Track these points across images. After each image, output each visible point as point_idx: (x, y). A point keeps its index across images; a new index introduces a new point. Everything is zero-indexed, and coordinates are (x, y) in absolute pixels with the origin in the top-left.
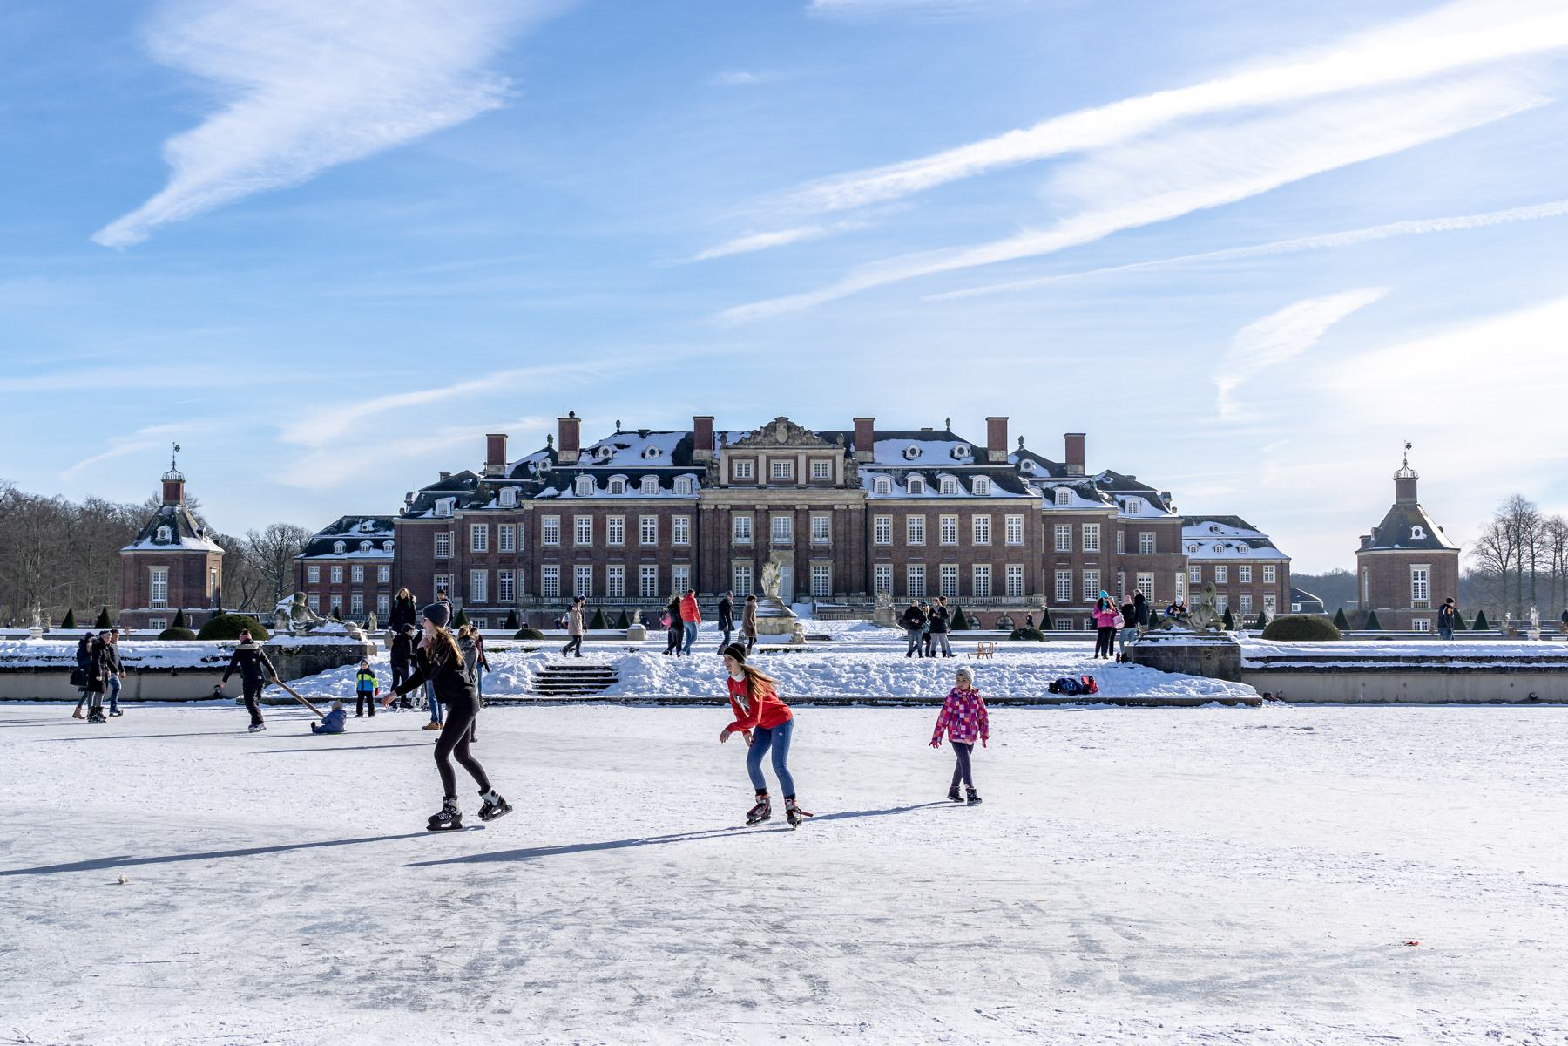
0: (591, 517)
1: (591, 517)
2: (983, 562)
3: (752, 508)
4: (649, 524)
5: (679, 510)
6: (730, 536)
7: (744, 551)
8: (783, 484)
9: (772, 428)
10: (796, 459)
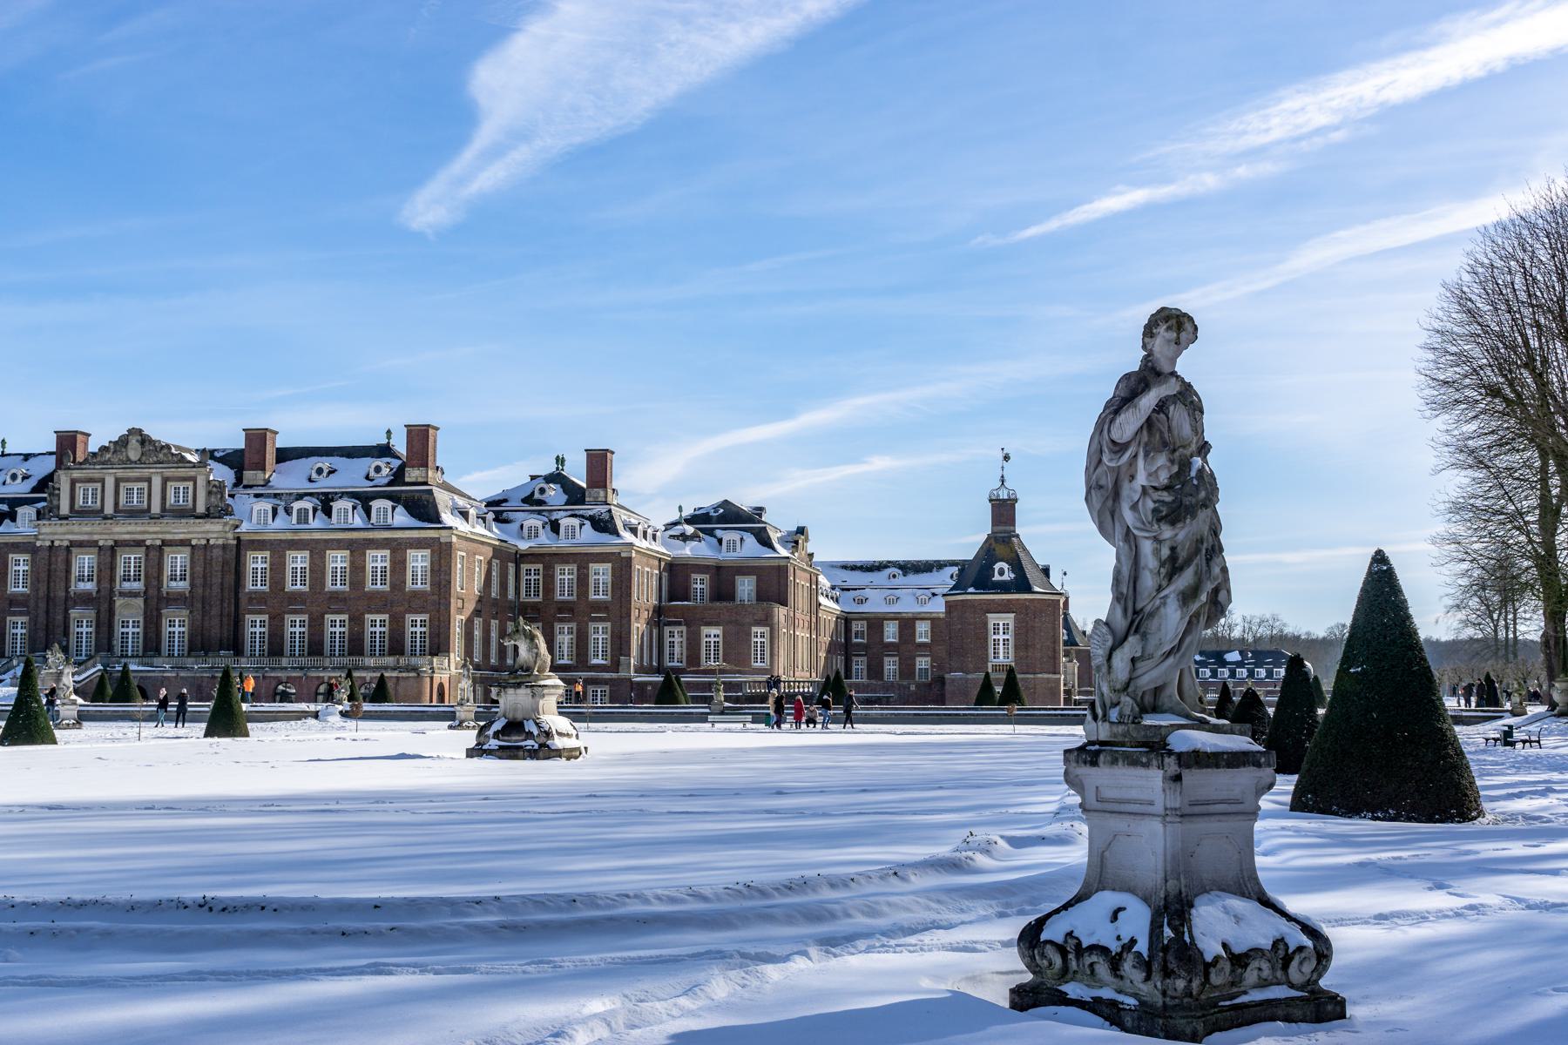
2: (378, 612)
3: (94, 544)
6: (68, 580)
7: (85, 599)
9: (122, 443)
10: (149, 481)
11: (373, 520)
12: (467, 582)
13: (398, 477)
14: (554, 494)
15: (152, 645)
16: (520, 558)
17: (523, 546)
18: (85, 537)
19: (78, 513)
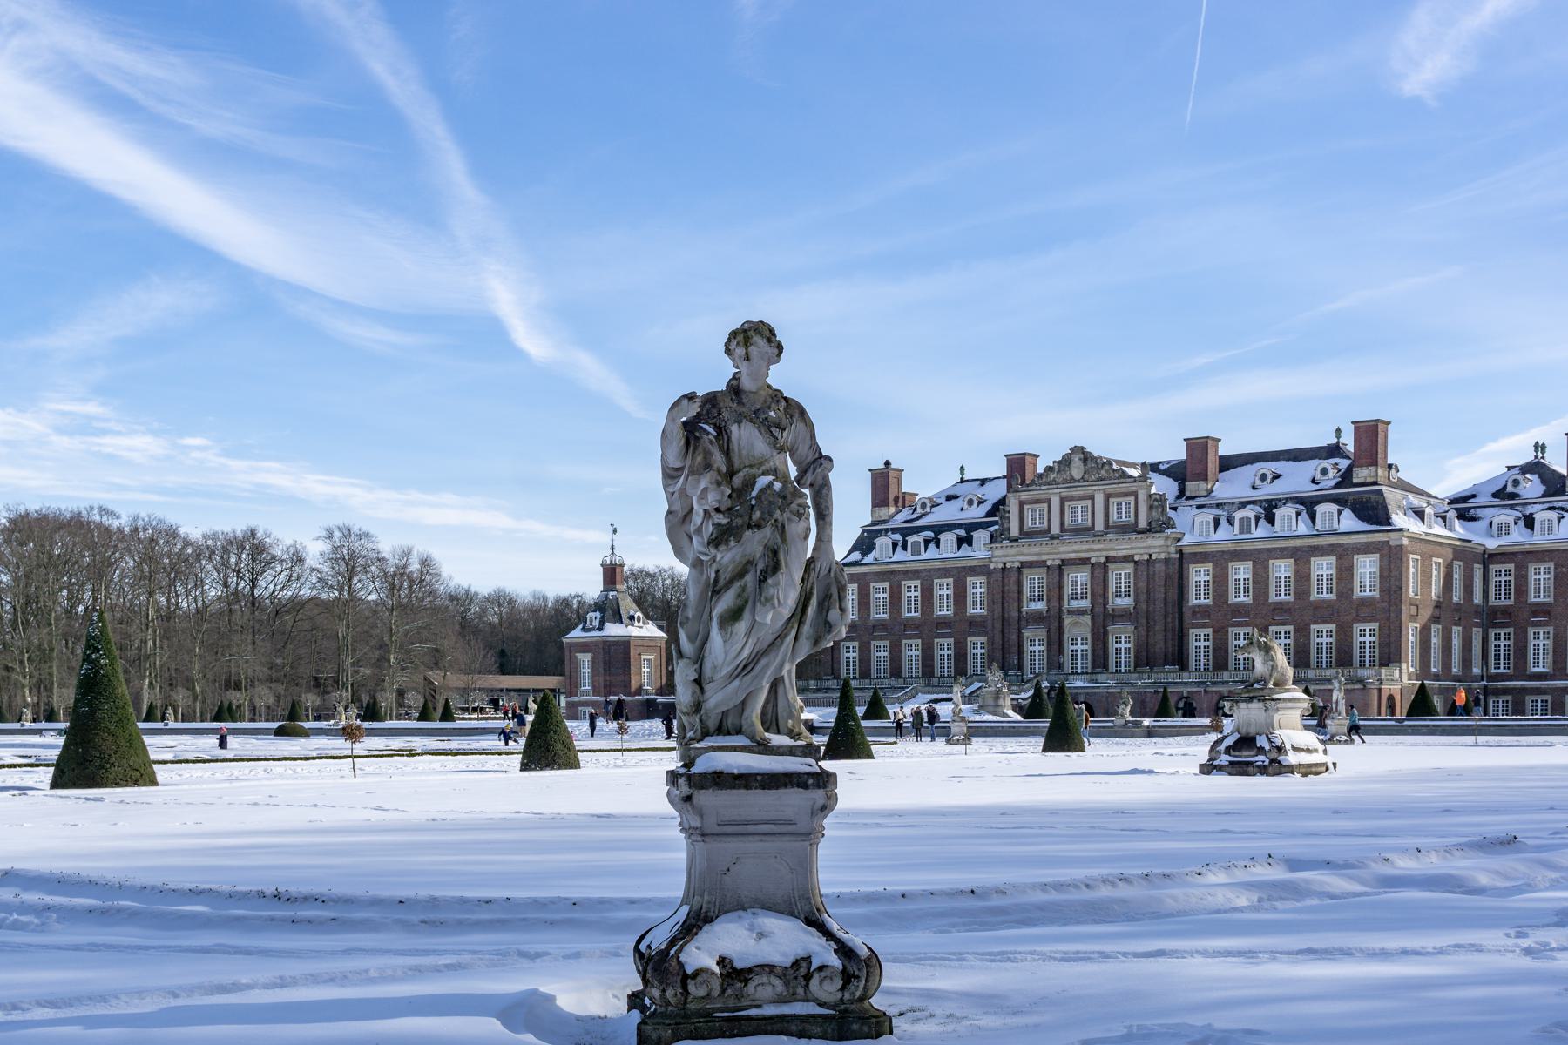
0: (886, 584)
1: (886, 584)
3: (1042, 564)
4: (944, 589)
5: (973, 571)
6: (1020, 600)
7: (1037, 618)
8: (1079, 532)
9: (1066, 462)
10: (1092, 498)
11: (1318, 526)
12: (1422, 584)
13: (1346, 479)
14: (1532, 487)
15: (1100, 661)
16: (1488, 558)
17: (1492, 544)
18: (1034, 558)
19: (1026, 534)
